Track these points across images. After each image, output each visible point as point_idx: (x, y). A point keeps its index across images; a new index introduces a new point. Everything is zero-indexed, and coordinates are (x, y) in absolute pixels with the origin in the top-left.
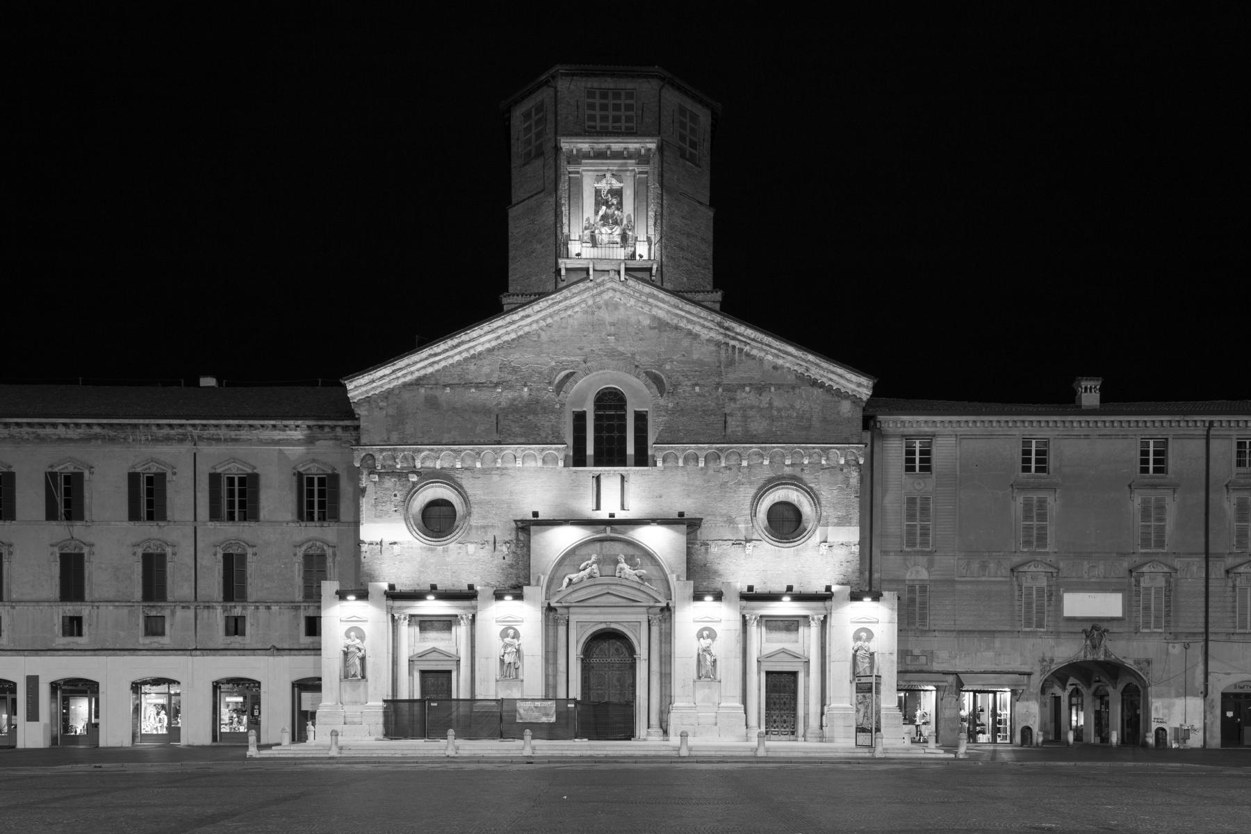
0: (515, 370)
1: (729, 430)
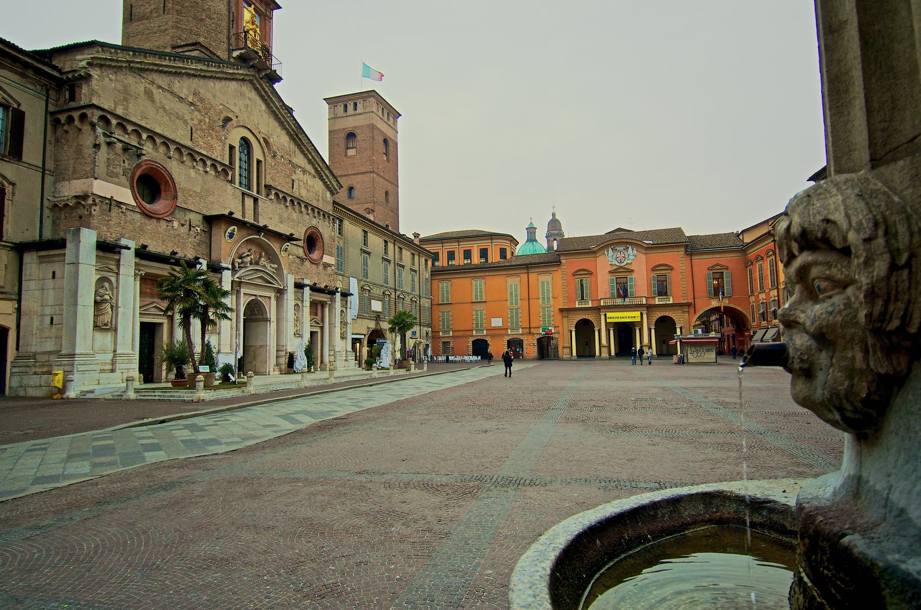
0: (202, 100)
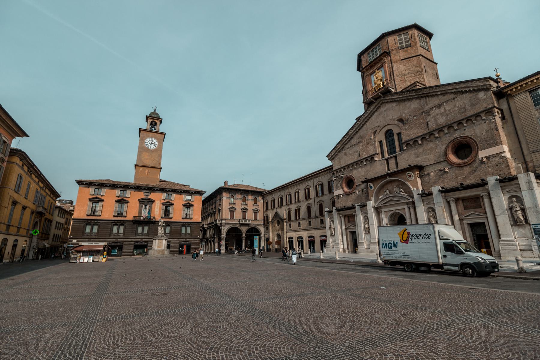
1: (430, 127)
